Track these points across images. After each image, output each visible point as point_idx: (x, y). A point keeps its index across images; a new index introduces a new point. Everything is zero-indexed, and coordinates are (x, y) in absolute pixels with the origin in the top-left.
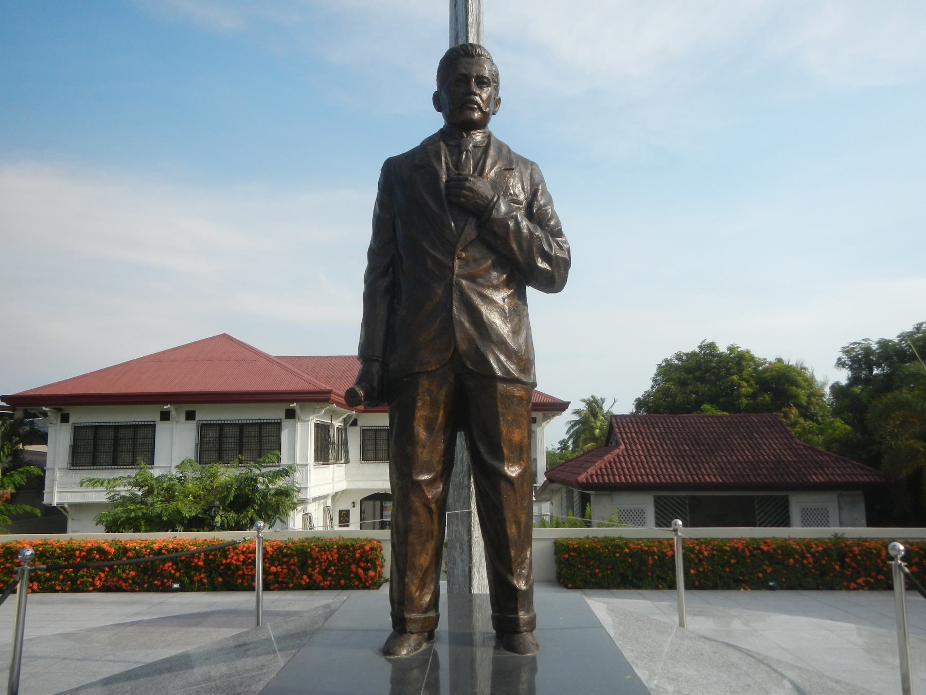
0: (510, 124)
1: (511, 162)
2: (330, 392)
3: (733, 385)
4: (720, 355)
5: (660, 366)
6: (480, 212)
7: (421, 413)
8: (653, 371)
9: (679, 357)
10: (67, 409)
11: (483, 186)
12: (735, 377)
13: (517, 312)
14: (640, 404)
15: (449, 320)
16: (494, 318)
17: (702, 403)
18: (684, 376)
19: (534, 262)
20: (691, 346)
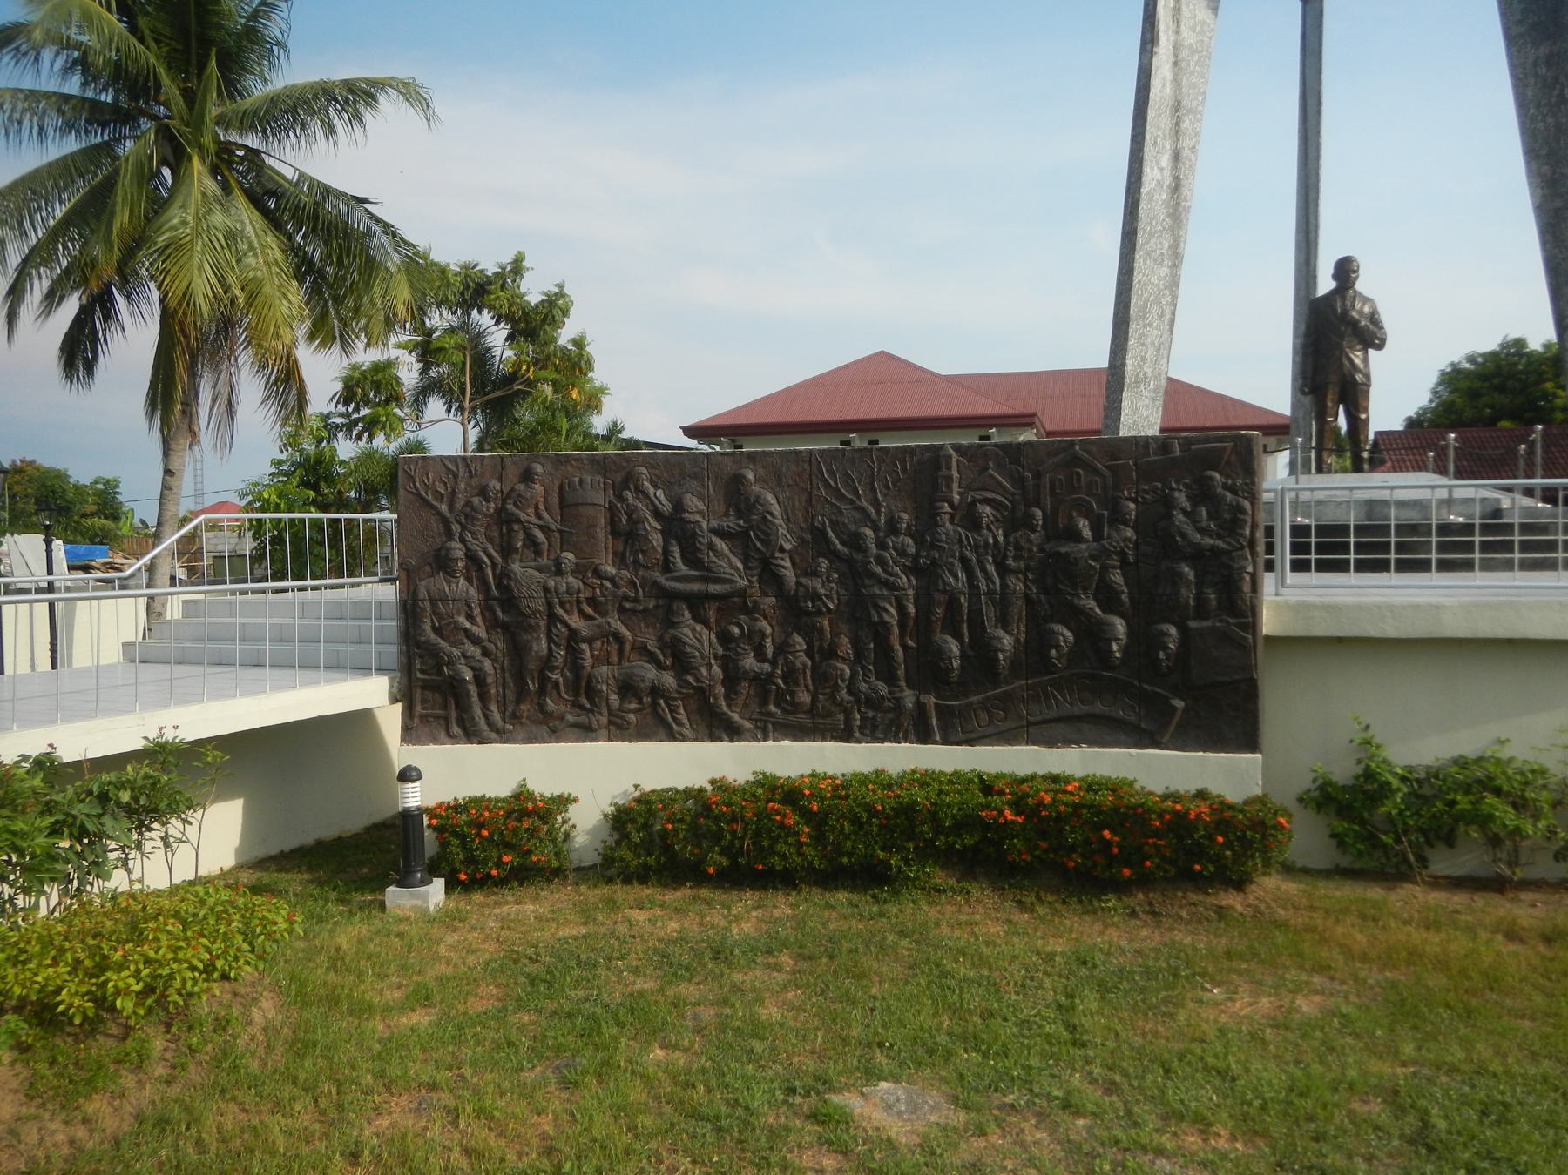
0: (1362, 286)
1: (1366, 300)
2: (1034, 415)
3: (1545, 396)
4: (1531, 354)
5: (1443, 373)
6: (1354, 324)
7: (1330, 397)
8: (1432, 379)
9: (1471, 359)
10: (740, 440)
11: (1354, 314)
12: (1549, 385)
13: (1366, 360)
14: (1412, 423)
15: (1342, 364)
16: (1357, 361)
17: (1500, 419)
18: (1477, 384)
19: (1371, 337)
20: (1488, 343)
